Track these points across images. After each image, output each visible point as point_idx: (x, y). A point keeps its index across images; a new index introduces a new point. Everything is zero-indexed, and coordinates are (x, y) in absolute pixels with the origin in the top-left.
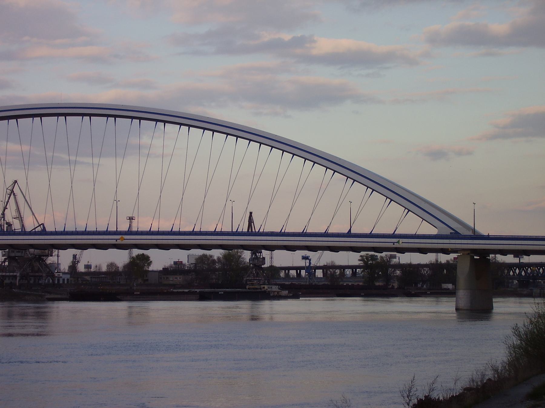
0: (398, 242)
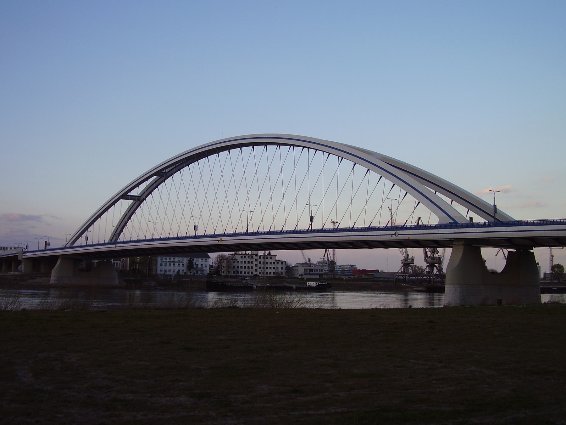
0: (395, 234)
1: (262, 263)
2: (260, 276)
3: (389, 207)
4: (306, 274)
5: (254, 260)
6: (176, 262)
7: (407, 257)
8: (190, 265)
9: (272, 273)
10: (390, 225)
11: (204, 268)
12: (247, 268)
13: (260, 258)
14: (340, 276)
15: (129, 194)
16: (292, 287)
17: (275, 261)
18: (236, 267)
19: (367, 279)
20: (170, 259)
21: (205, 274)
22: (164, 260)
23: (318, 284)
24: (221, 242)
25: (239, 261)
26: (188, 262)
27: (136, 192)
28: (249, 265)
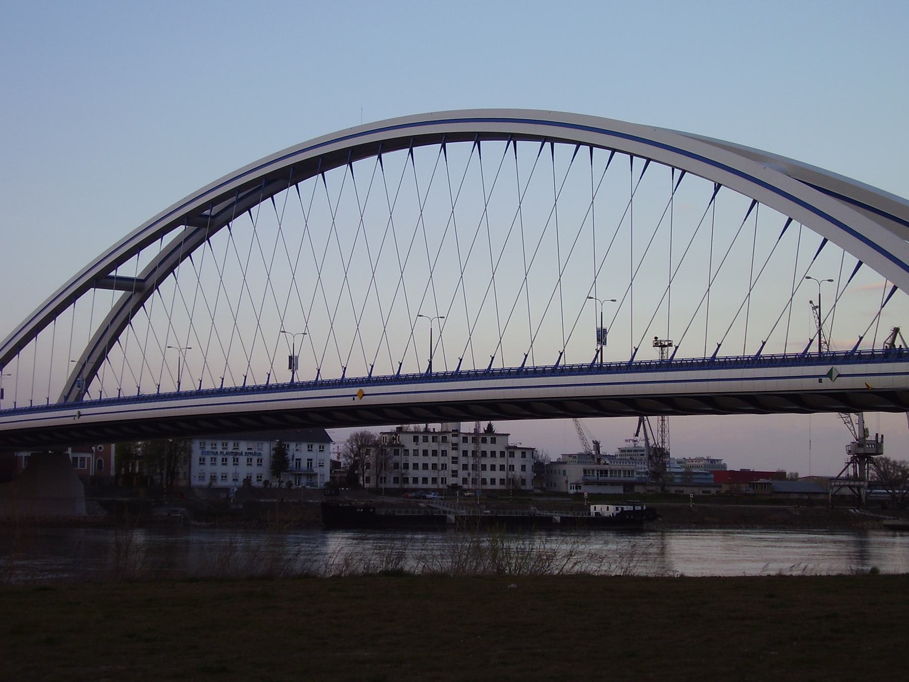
0: (829, 375)
1: (470, 454)
2: (466, 491)
3: (811, 302)
4: (587, 483)
5: (447, 447)
7: (863, 436)
8: (280, 463)
9: (498, 482)
10: (814, 349)
11: (316, 470)
12: (430, 467)
13: (465, 440)
14: (681, 489)
15: (113, 273)
16: (551, 518)
17: (504, 450)
18: (401, 465)
19: (754, 495)
20: (225, 446)
21: (319, 485)
22: (210, 450)
23: (620, 509)
24: (361, 399)
25: (408, 450)
26: (273, 452)
27: (131, 269)
28: (434, 460)
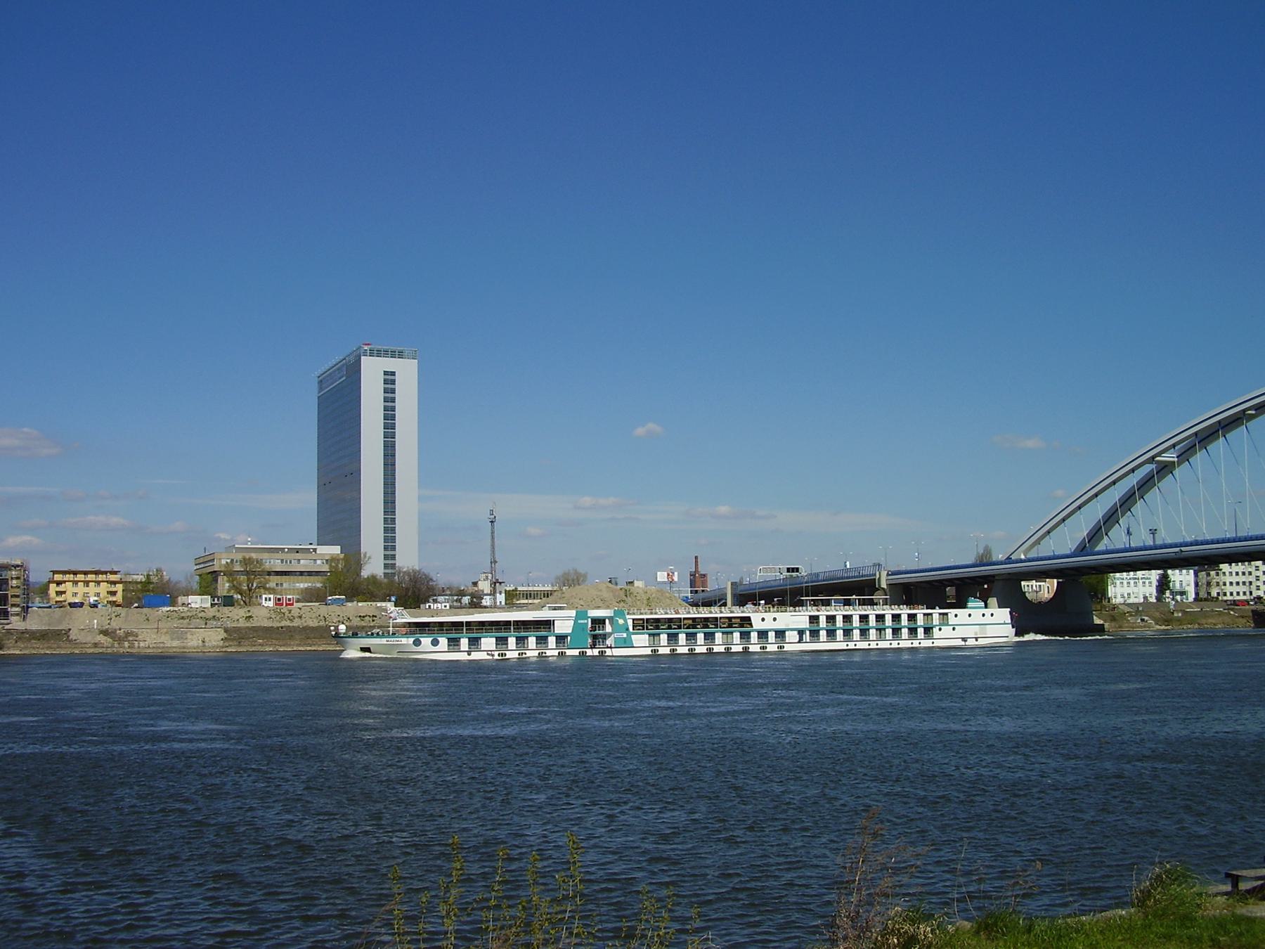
5: (1252, 569)
6: (1142, 579)
8: (1163, 584)
18: (1221, 583)
